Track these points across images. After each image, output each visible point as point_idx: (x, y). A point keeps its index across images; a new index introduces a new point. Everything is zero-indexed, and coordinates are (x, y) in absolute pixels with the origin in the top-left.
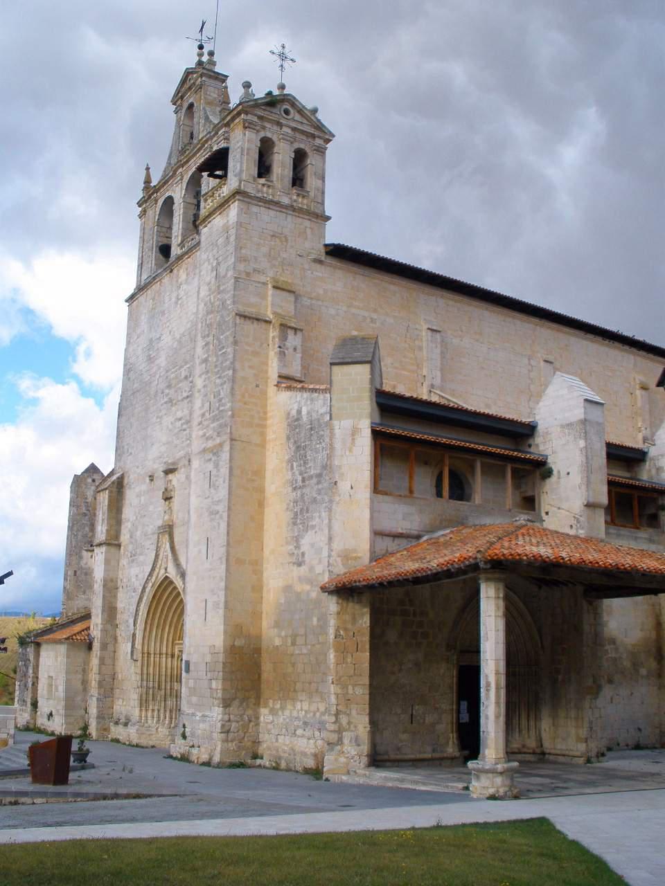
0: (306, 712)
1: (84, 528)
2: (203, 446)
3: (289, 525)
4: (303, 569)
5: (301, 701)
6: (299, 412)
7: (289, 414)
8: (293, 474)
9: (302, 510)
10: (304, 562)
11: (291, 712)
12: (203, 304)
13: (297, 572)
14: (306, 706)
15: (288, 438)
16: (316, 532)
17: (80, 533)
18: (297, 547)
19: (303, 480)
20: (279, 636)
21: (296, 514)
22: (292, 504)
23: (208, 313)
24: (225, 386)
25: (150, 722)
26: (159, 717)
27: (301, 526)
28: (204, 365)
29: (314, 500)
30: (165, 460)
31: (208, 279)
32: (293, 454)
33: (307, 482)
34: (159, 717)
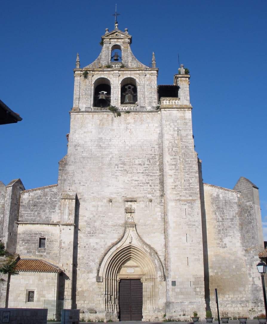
0: (232, 298)
1: (15, 211)
2: (178, 198)
3: (215, 233)
4: (225, 249)
5: (228, 295)
6: (218, 195)
7: (212, 195)
8: (217, 216)
9: (222, 229)
10: (226, 247)
11: (223, 299)
12: (168, 142)
13: (222, 250)
14: (231, 296)
15: (212, 203)
16: (232, 237)
17: (13, 214)
18: (222, 241)
19: (223, 219)
20: (213, 272)
21: (220, 230)
22: (217, 226)
23: (173, 147)
24: (193, 179)
25: (109, 310)
26: (112, 308)
27: (223, 235)
28: (174, 167)
29: (230, 227)
30: (123, 195)
31: (172, 133)
32: (215, 209)
33: (225, 220)
34: (112, 308)
